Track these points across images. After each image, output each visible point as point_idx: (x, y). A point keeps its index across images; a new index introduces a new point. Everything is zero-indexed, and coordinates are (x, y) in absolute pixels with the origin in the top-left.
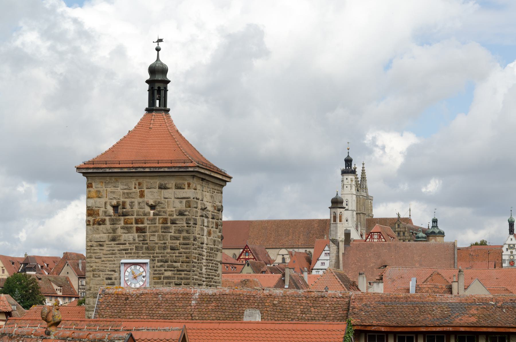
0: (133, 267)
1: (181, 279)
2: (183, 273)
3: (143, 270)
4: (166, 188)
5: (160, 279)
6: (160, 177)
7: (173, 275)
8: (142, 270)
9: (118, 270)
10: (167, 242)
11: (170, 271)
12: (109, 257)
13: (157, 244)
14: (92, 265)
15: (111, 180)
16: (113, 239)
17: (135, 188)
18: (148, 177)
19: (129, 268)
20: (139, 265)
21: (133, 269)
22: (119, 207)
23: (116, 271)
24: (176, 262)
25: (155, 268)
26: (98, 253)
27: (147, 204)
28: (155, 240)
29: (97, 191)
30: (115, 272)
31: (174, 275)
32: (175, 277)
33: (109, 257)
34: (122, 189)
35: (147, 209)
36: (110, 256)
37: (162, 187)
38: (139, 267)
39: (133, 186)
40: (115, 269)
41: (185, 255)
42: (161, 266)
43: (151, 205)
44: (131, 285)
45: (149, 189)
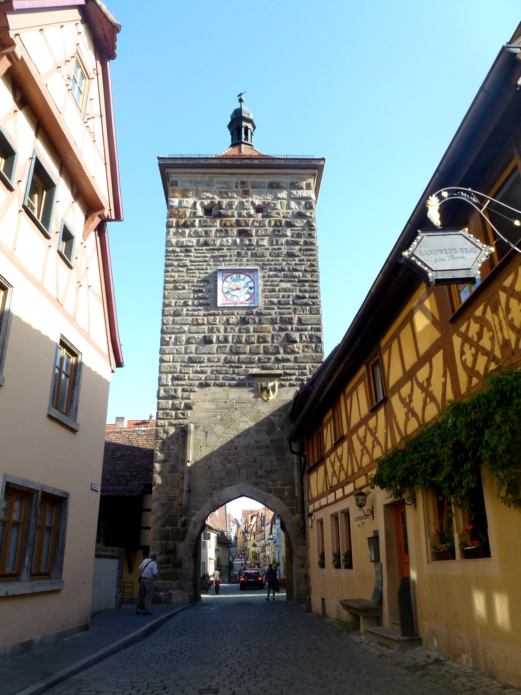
0: (235, 276)
1: (305, 291)
2: (307, 284)
3: (250, 280)
4: (280, 187)
5: (274, 291)
6: (271, 176)
7: (293, 287)
8: (248, 279)
9: (212, 280)
10: (283, 247)
11: (289, 281)
12: (199, 265)
13: (268, 249)
14: (173, 274)
15: (203, 178)
16: (206, 244)
17: (236, 187)
18: (254, 176)
19: (229, 278)
20: (244, 274)
21: (235, 278)
22: (213, 209)
23: (210, 281)
24: (296, 270)
25: (266, 279)
26: (183, 260)
27: (253, 203)
28: (265, 244)
29: (184, 189)
30: (208, 283)
31: (295, 286)
32: (296, 289)
33: (199, 265)
34: (219, 188)
35: (252, 212)
36: (201, 264)
37: (274, 185)
38: (244, 276)
39: (234, 185)
40: (208, 279)
41: (309, 263)
42: (276, 276)
43: (259, 207)
44: (232, 299)
45: (256, 188)
